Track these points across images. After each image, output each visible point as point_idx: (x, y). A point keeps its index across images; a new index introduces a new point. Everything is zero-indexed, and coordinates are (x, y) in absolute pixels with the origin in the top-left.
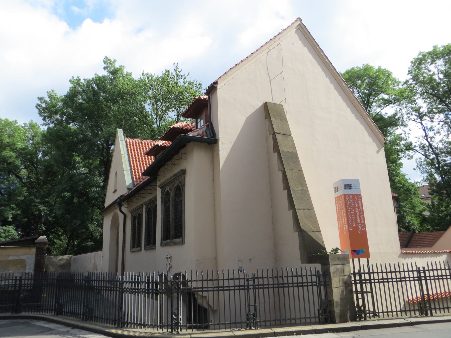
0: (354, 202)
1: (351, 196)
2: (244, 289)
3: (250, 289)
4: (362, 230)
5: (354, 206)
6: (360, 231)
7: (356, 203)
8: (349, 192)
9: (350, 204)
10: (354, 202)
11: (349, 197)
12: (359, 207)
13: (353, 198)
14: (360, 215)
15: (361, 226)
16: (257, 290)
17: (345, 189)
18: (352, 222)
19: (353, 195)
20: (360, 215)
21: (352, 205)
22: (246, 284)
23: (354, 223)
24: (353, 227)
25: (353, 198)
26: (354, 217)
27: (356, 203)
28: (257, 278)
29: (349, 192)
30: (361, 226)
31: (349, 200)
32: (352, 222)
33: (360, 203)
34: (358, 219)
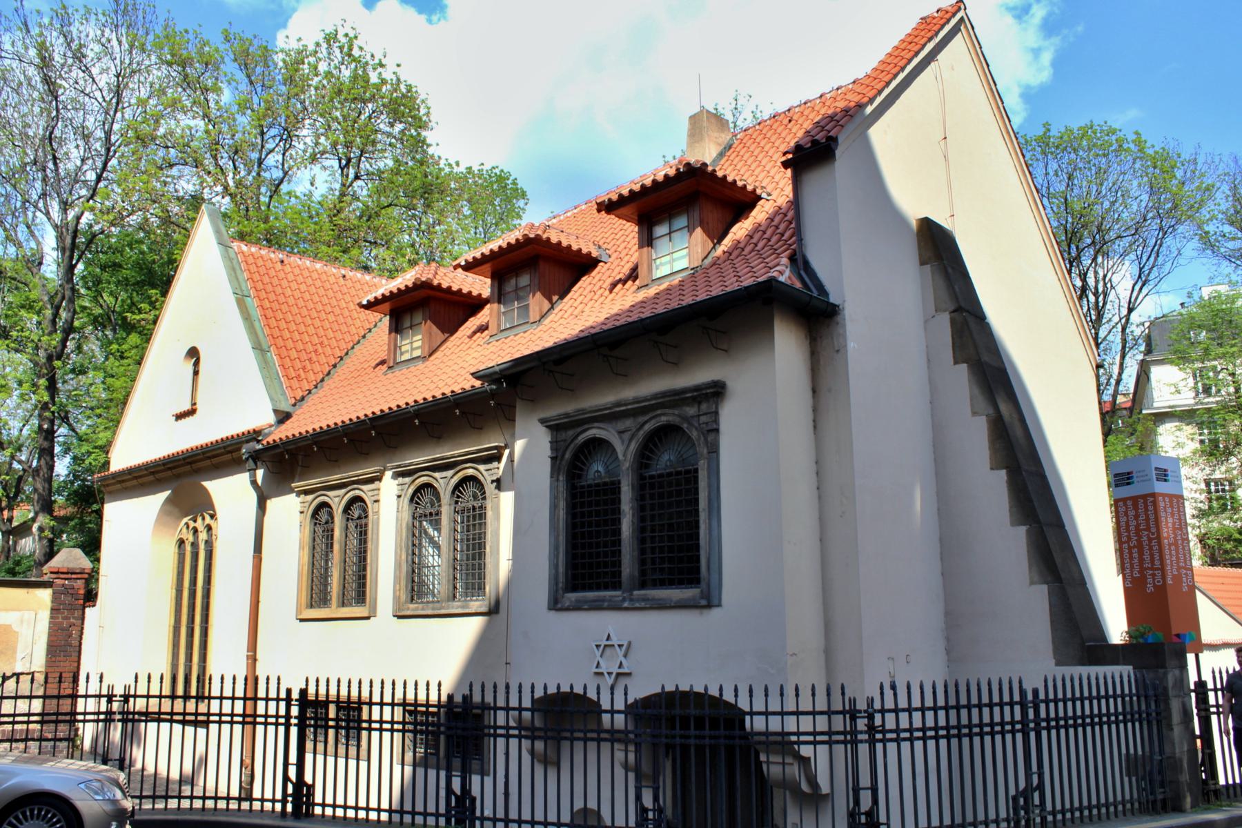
0: (1136, 517)
1: (1129, 503)
2: (845, 742)
3: (861, 741)
4: (1155, 586)
5: (1138, 526)
6: (1150, 588)
7: (1142, 517)
8: (1126, 492)
9: (1127, 523)
10: (1136, 517)
11: (1125, 505)
12: (1148, 529)
13: (1136, 507)
14: (1151, 548)
15: (1153, 575)
16: (879, 746)
17: (1117, 486)
18: (1132, 565)
19: (1134, 499)
20: (1151, 548)
21: (1133, 523)
22: (848, 728)
23: (1137, 568)
24: (1134, 580)
25: (1136, 507)
26: (1136, 555)
27: (1142, 517)
28: (879, 711)
29: (1126, 492)
30: (1153, 575)
31: (1126, 514)
33: (1152, 517)
34: (1147, 557)
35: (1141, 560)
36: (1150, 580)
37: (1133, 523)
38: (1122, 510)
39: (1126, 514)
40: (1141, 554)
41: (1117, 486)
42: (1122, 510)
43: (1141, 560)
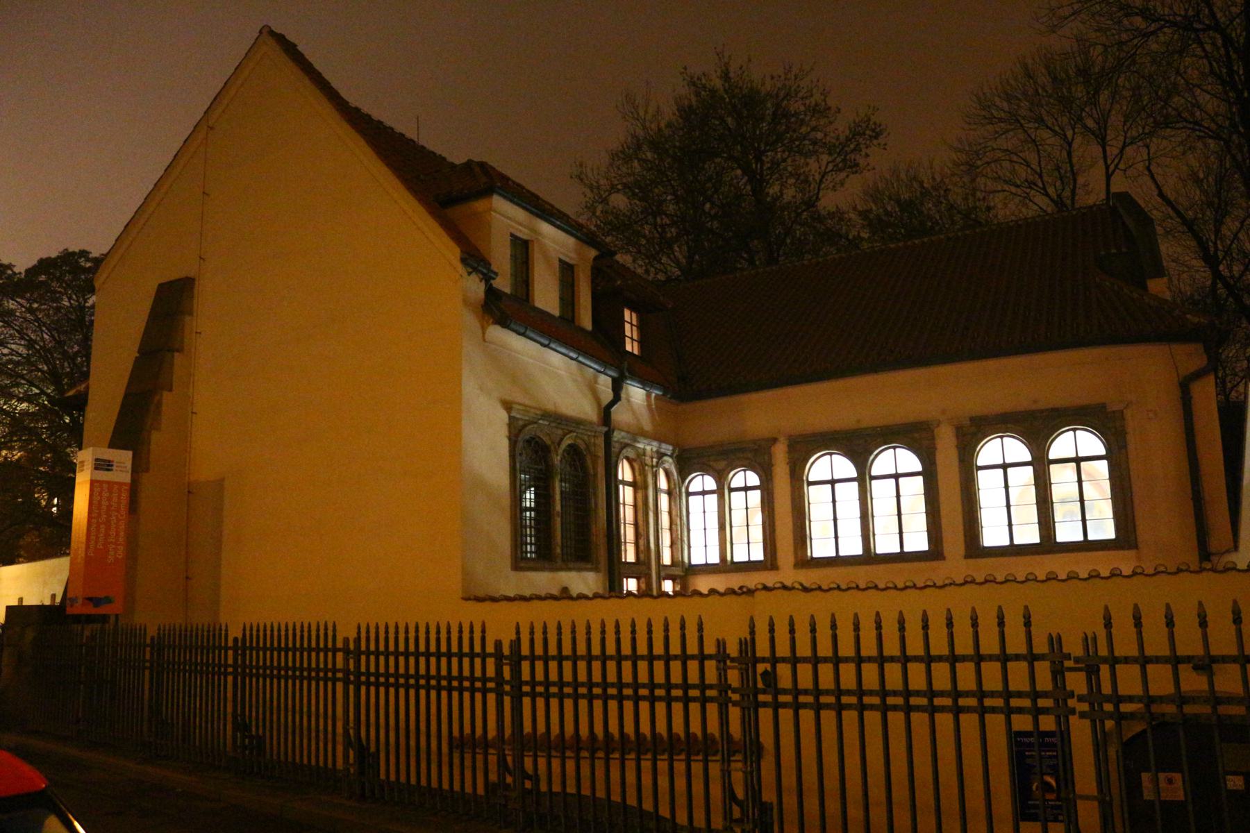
0: (109, 499)
5: (109, 506)
6: (111, 559)
7: (115, 499)
8: (103, 476)
10: (109, 499)
15: (116, 550)
17: (96, 468)
18: (97, 538)
21: (105, 503)
25: (110, 490)
26: (103, 530)
27: (115, 499)
31: (100, 494)
32: (97, 538)
34: (113, 533)
35: (107, 535)
36: (112, 553)
37: (105, 503)
38: (97, 490)
39: (100, 494)
40: (108, 528)
41: (96, 468)
42: (97, 490)
43: (107, 535)
